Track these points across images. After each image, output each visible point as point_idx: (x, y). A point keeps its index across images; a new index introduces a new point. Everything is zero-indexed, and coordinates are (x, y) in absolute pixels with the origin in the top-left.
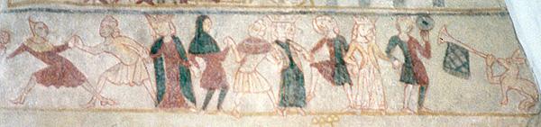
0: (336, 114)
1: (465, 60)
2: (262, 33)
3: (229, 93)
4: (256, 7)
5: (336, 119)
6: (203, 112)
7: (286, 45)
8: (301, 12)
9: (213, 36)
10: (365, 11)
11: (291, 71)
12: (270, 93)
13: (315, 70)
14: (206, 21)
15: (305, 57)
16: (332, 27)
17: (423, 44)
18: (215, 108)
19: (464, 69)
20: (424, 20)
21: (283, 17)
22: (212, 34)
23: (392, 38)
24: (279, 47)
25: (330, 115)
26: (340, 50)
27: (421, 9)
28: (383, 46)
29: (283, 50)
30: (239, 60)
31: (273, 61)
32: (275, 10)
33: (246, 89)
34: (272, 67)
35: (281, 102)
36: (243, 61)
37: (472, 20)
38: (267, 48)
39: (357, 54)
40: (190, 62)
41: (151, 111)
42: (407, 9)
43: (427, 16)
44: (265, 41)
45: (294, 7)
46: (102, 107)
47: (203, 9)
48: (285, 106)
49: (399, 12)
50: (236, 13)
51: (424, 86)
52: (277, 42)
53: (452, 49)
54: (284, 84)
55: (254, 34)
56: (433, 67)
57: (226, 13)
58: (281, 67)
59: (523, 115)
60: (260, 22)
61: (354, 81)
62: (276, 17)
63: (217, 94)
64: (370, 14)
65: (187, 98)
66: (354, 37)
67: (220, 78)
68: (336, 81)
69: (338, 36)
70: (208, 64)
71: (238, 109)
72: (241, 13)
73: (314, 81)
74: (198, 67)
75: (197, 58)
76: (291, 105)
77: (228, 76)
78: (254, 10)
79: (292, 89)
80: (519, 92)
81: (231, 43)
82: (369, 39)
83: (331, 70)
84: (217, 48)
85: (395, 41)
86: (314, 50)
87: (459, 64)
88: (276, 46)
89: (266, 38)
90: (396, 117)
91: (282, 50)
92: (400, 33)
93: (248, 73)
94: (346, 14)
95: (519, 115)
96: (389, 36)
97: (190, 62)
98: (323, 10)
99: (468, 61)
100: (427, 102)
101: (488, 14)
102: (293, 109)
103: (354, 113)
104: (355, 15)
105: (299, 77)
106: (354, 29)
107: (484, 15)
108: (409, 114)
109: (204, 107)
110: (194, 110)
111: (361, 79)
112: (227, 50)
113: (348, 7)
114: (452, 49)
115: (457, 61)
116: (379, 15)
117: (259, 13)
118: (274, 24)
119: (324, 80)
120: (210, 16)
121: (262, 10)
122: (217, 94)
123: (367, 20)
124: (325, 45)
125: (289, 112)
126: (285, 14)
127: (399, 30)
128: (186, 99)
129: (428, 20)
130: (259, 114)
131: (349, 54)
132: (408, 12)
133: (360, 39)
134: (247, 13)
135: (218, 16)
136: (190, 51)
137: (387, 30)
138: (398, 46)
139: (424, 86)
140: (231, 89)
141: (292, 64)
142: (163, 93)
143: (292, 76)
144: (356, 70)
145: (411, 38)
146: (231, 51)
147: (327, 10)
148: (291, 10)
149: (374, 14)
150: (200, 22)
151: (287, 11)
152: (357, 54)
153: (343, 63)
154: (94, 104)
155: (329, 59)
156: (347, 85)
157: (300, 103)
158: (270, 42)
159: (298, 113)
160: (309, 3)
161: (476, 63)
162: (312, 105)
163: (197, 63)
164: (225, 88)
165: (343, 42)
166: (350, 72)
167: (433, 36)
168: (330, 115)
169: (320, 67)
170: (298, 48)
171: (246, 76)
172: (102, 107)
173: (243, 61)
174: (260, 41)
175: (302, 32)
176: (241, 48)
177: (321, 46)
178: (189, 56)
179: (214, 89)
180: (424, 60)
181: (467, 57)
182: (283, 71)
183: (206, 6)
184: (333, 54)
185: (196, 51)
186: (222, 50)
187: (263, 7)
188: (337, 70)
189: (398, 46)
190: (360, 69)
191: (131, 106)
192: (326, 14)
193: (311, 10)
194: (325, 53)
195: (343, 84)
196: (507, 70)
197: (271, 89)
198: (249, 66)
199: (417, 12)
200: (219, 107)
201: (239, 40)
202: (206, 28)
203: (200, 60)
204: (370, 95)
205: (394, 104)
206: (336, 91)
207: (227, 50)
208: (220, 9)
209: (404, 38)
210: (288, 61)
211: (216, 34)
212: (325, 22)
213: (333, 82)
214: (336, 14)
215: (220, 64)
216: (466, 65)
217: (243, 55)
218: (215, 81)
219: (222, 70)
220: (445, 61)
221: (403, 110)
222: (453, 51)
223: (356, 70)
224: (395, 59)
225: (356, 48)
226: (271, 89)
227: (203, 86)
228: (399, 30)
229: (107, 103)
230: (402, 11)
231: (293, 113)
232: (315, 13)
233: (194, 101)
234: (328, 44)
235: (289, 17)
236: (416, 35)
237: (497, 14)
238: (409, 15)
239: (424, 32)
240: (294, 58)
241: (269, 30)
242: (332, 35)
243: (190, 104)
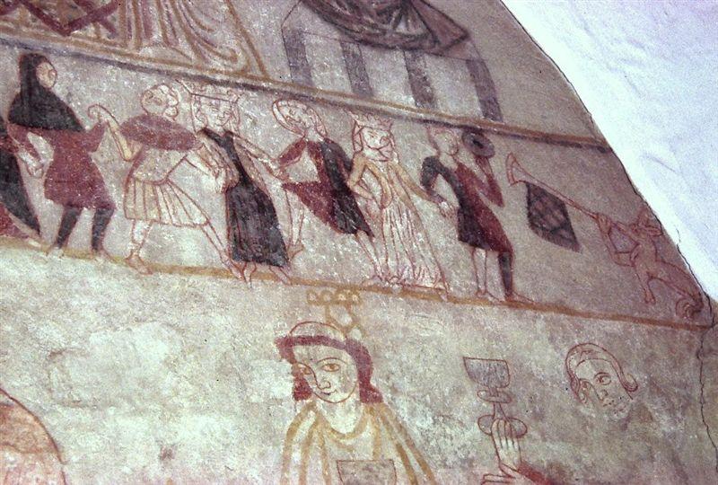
0: (354, 289)
1: (561, 217)
2: (170, 111)
3: (116, 219)
4: (149, 59)
5: (355, 297)
6: (57, 251)
7: (226, 141)
8: (245, 86)
9: (63, 98)
10: (368, 104)
11: (245, 193)
12: (207, 228)
13: (294, 199)
14: (44, 66)
15: (270, 171)
16: (317, 123)
17: (484, 179)
18: (89, 247)
19: (564, 233)
20: (475, 137)
21: (210, 88)
22: (59, 90)
23: (427, 159)
24: (213, 143)
25: (340, 289)
26: (337, 165)
27: (466, 119)
28: (414, 171)
29: (223, 151)
30: (128, 154)
31: (205, 169)
32: (191, 72)
34: (205, 180)
35: (235, 250)
36: (138, 160)
37: (556, 152)
38: (185, 142)
39: (367, 177)
40: (16, 142)
42: (441, 115)
43: (480, 132)
44: (178, 127)
45: (227, 73)
47: (31, 41)
48: (247, 261)
49: (429, 117)
50: (108, 62)
51: (506, 254)
52: (207, 132)
53: (535, 195)
54: (234, 216)
55: (153, 109)
56: (512, 220)
57: (88, 59)
58: (221, 181)
59: (687, 327)
60: (164, 88)
61: (374, 227)
62: (197, 84)
63: (87, 217)
64: (378, 112)
66: (358, 148)
67: (91, 184)
68: (340, 223)
69: (327, 140)
70: (58, 151)
71: (143, 253)
72: (121, 65)
73: (296, 219)
74: (35, 155)
75: (30, 136)
76: (259, 260)
77: (107, 184)
78: (147, 64)
79: (253, 236)
80: (665, 282)
81: (106, 118)
82: (387, 155)
83: (325, 203)
84: (77, 125)
85: (432, 168)
86: (289, 157)
87: (555, 223)
88: (204, 140)
89: (180, 121)
90: (468, 307)
91: (218, 148)
92: (439, 153)
93: (154, 184)
94: (334, 104)
95: (682, 326)
96: (422, 157)
97: (16, 142)
98: (288, 89)
99: (568, 219)
100: (519, 284)
101: (579, 146)
102: (263, 268)
103: (387, 291)
104: (350, 108)
105: (264, 207)
106: (355, 134)
107: (572, 145)
108: (491, 304)
109: (63, 238)
110: (33, 243)
111: (387, 226)
112: (99, 129)
113: (335, 94)
114: (535, 195)
115: (550, 217)
116: (394, 116)
117: (159, 72)
118: (191, 97)
119: (316, 219)
120: (52, 57)
121: (165, 67)
122: (87, 217)
123: (374, 122)
124: (305, 153)
125: (254, 274)
126: (213, 82)
127: (436, 147)
128: (12, 217)
129: (480, 140)
130: (192, 270)
131: (355, 177)
132: (446, 120)
133: (368, 152)
134: (131, 67)
135: (67, 61)
136: (12, 119)
137: (413, 151)
138: (440, 177)
139: (506, 254)
140: (120, 210)
141: (245, 180)
143: (247, 206)
144: (374, 208)
145: (461, 166)
146: (107, 134)
147: (296, 91)
148: (225, 78)
149: (385, 114)
150: (30, 63)
151: (218, 78)
152: (367, 177)
153: (349, 192)
155: (316, 179)
156: (362, 236)
157: (275, 256)
158: (190, 128)
159: (277, 279)
160: (258, 73)
161: (583, 227)
162: (299, 263)
163: (31, 146)
164: (104, 212)
165: (339, 153)
166: (364, 212)
167: (497, 165)
168: (340, 289)
169: (302, 191)
170: (253, 151)
171: (149, 188)
173: (138, 160)
174: (168, 124)
175: (254, 123)
176: (128, 130)
177: (299, 154)
178: (12, 129)
179: (79, 207)
180: (493, 207)
181: (565, 214)
182: (228, 190)
183: (37, 36)
184: (324, 171)
185: (27, 119)
186: (88, 128)
187: (163, 62)
188: (337, 200)
189: (440, 177)
190: (382, 207)
192: (293, 97)
193: (264, 84)
194: (307, 168)
195: (355, 232)
196: (637, 244)
197: (208, 222)
198: (153, 170)
199: (459, 122)
200: (96, 244)
201: (124, 117)
202: (44, 77)
203: (41, 143)
204: (412, 260)
205: (460, 281)
206: (343, 243)
207: (99, 129)
208: (73, 48)
209: (448, 162)
210: (236, 173)
211: (70, 95)
212: (298, 111)
213: (334, 225)
214: (316, 101)
215: (87, 162)
216: (566, 225)
217: (138, 147)
218: (79, 188)
219: (91, 169)
220: (530, 215)
221: (480, 296)
222: (539, 198)
223: (374, 208)
224: (442, 199)
225: (365, 168)
226: (208, 222)
227: (51, 195)
228: (436, 147)
230: (433, 117)
231: (262, 277)
232: (272, 91)
233: (34, 224)
234: (311, 153)
235: (224, 90)
236: (468, 160)
237: (592, 147)
238: (448, 125)
239: (482, 159)
240: (248, 169)
241: (185, 106)
242: (315, 137)
243: (26, 230)
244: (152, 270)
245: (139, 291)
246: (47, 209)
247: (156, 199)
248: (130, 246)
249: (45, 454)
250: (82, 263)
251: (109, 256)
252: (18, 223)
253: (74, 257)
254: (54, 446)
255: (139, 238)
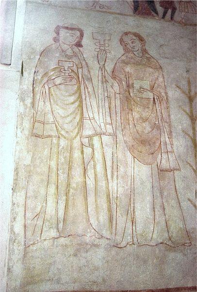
18: (170, 19)
33: (186, 11)
41: (130, 15)
46: (101, 10)
63: (170, 11)
65: (153, 11)
122: (170, 11)
140: (178, 9)
142: (138, 7)
154: (95, 7)
172: (101, 10)
179: (168, 9)
191: (118, 12)
200: (172, 18)
227: (161, 6)
229: (103, 8)
233: (157, 13)
243: (155, 15)
244: (185, 25)
245: (182, 30)
246: (160, 10)
247: (187, 6)
248: (180, 19)
249: (159, 69)
250: (168, 23)
251: (175, 21)
252: (153, 13)
253: (166, 21)
254: (161, 68)
255: (182, 17)
